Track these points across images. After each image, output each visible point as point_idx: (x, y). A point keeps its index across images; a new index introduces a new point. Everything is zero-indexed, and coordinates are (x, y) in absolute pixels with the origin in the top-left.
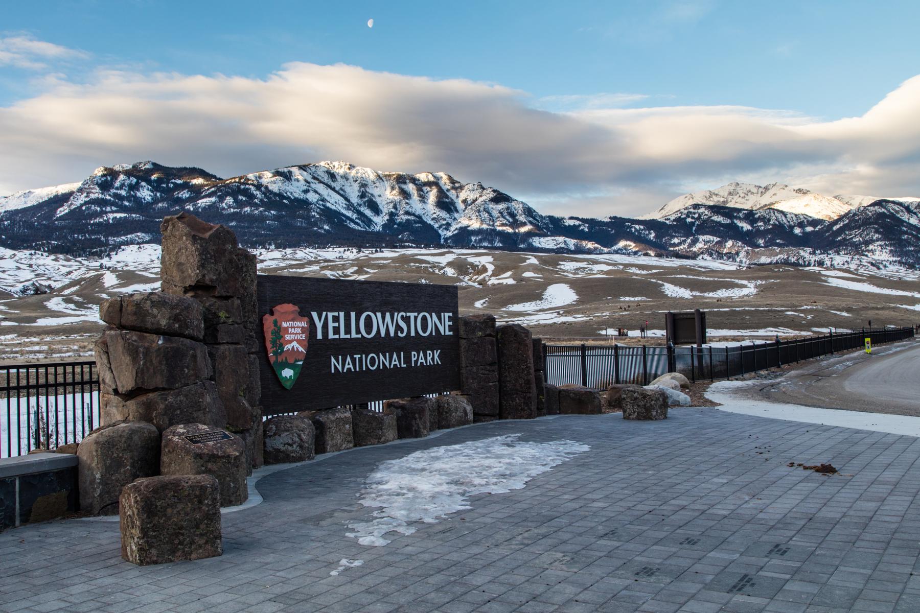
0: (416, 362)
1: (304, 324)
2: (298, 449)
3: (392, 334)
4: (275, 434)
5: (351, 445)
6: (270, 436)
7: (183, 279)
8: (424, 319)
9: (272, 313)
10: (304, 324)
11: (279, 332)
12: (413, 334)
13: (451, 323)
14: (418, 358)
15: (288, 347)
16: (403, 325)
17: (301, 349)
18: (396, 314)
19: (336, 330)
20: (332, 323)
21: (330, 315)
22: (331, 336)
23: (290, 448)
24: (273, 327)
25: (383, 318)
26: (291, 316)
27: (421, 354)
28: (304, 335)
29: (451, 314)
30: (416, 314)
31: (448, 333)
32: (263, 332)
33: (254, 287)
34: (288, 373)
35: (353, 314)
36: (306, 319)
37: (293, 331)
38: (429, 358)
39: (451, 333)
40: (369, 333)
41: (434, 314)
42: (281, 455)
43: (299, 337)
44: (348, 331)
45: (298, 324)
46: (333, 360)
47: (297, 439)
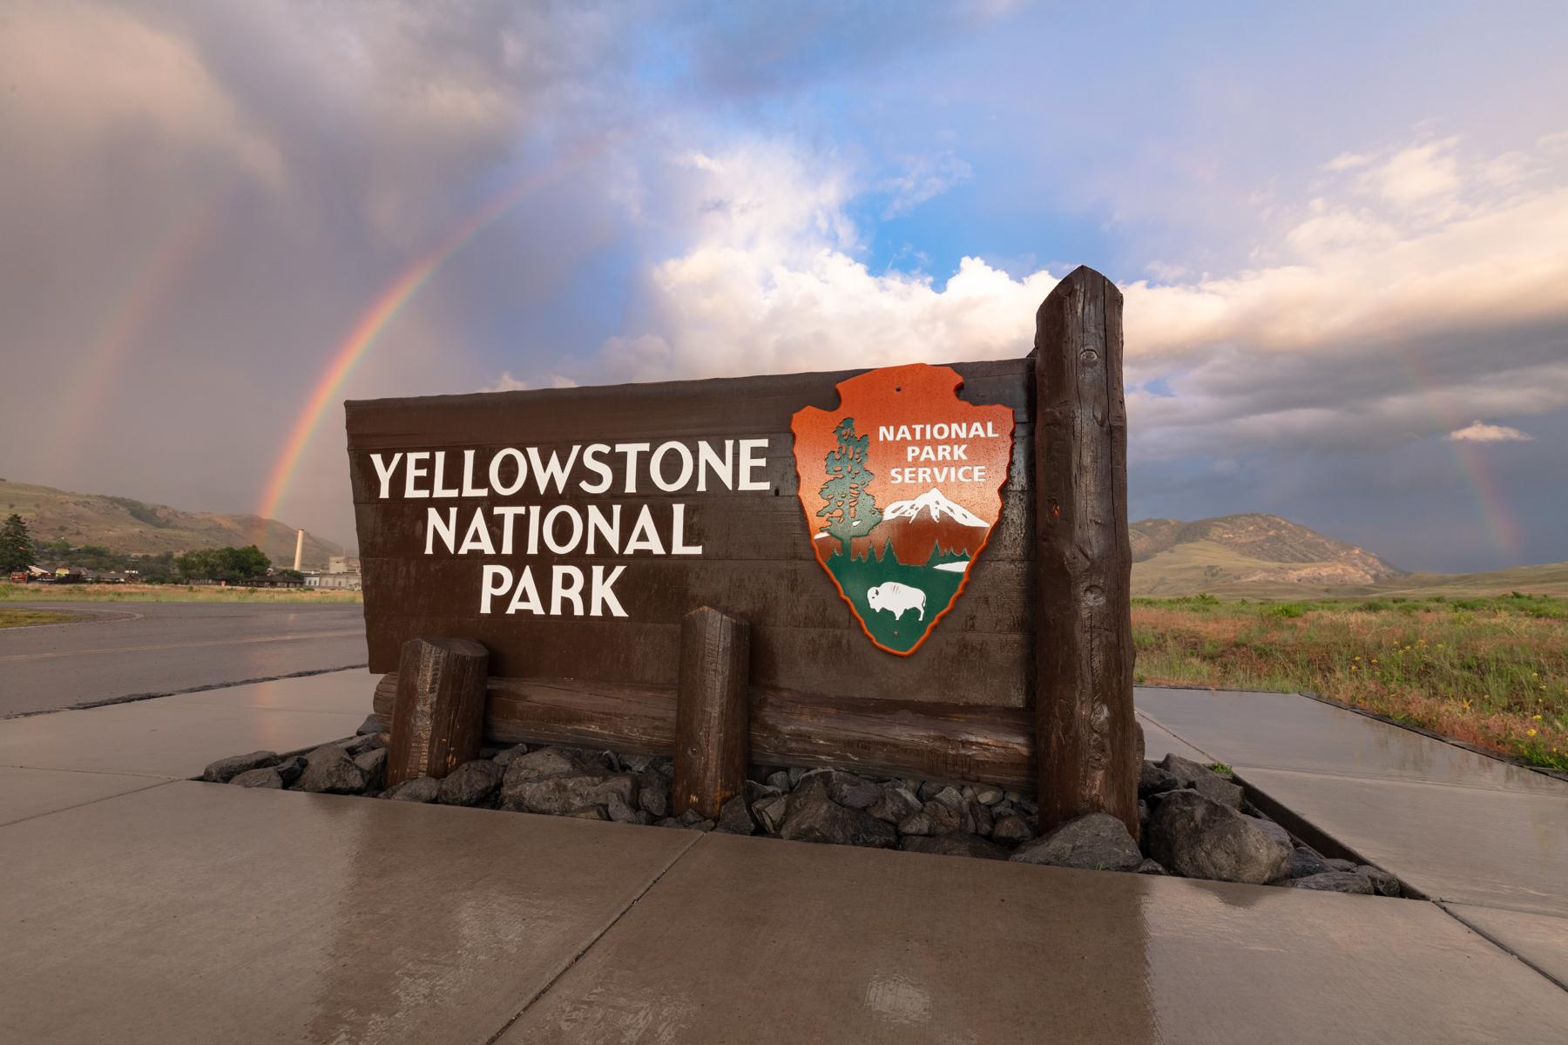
21: (412, 457)
22: (410, 492)
30: (645, 447)
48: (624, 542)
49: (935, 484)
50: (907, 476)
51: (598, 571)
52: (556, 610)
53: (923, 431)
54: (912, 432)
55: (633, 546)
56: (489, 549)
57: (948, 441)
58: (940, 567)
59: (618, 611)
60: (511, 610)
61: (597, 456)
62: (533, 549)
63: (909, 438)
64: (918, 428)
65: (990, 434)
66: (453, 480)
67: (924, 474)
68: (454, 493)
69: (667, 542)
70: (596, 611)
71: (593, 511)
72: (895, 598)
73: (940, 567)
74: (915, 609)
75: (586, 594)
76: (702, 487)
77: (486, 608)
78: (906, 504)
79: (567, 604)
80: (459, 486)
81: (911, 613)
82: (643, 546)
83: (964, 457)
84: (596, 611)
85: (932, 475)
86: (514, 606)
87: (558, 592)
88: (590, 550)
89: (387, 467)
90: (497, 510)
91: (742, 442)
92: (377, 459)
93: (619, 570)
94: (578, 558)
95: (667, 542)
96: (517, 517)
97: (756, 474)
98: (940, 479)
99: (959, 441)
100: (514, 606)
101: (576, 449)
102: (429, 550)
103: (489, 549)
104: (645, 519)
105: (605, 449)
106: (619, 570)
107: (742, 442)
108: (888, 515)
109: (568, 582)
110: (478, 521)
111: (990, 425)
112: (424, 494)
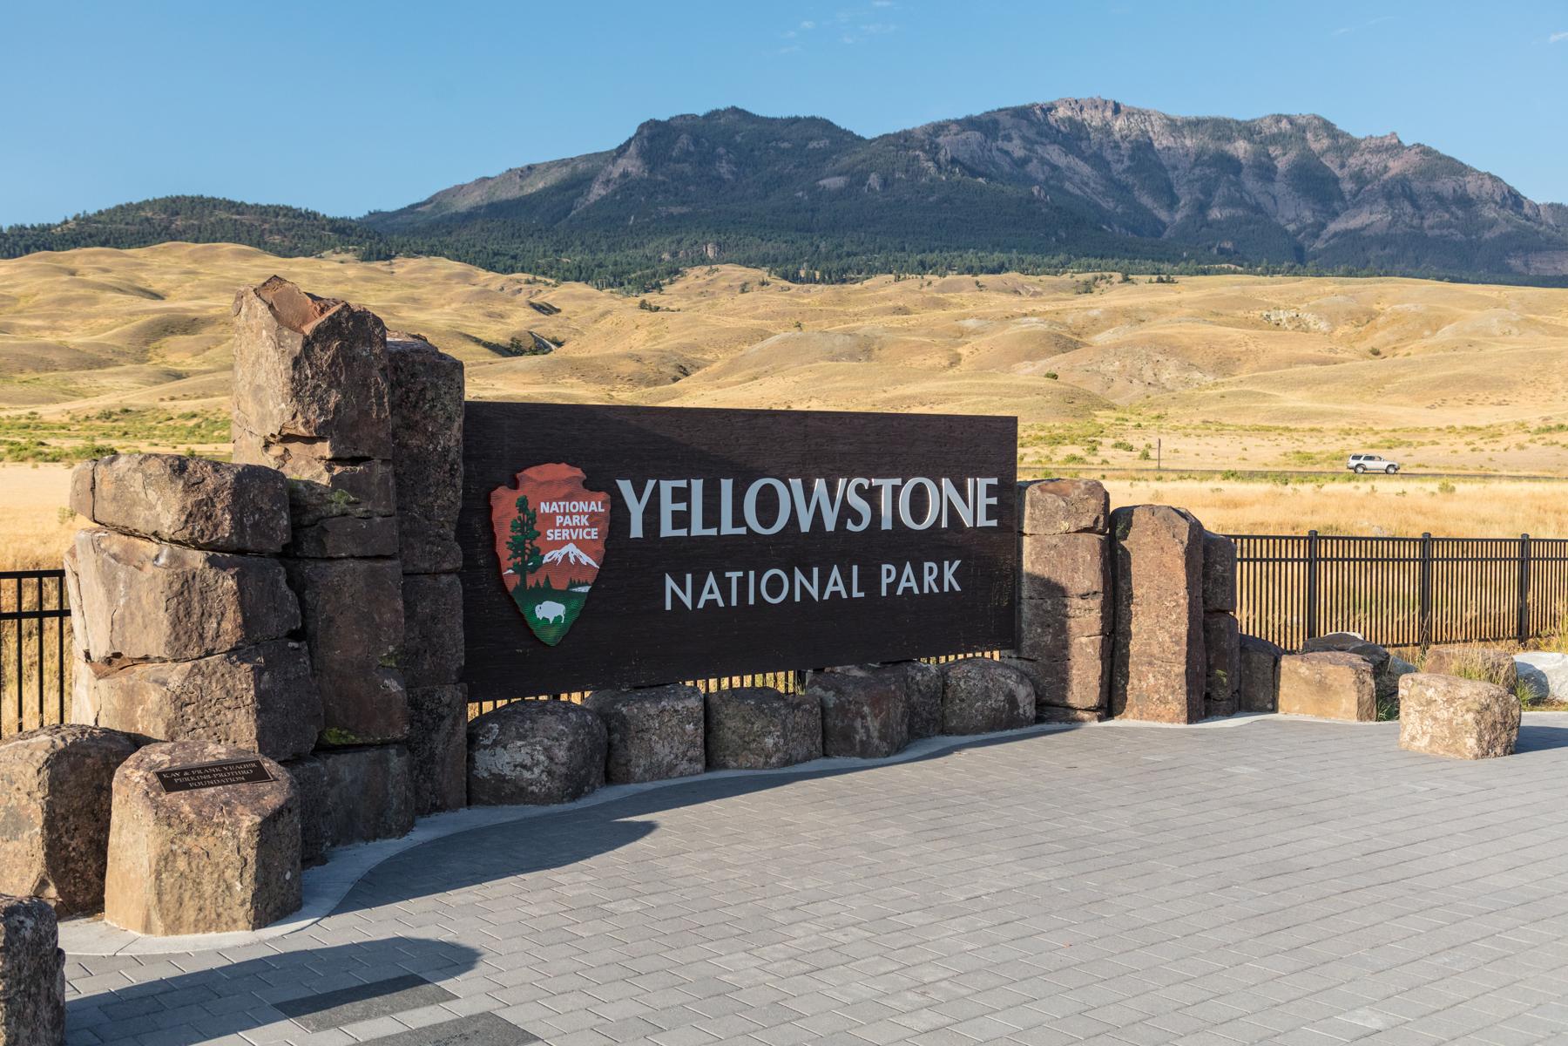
0: (893, 587)
1: (597, 506)
2: (544, 776)
3: (830, 526)
4: (495, 743)
5: (699, 767)
6: (485, 747)
7: (262, 420)
8: (919, 492)
9: (514, 484)
10: (597, 506)
11: (530, 525)
12: (887, 525)
13: (994, 501)
14: (896, 578)
15: (557, 555)
16: (861, 506)
17: (585, 559)
18: (841, 482)
19: (681, 520)
20: (669, 506)
21: (666, 487)
22: (667, 530)
23: (527, 775)
24: (515, 514)
25: (808, 491)
26: (566, 490)
27: (908, 569)
28: (594, 531)
29: (994, 481)
30: (898, 481)
31: (982, 521)
32: (490, 525)
33: (453, 436)
34: (550, 611)
35: (727, 486)
36: (603, 495)
37: (567, 521)
38: (929, 580)
39: (994, 523)
40: (767, 521)
41: (945, 482)
42: (508, 789)
43: (583, 534)
44: (712, 517)
45: (582, 506)
46: (670, 583)
47: (542, 758)
76: (944, 524)
80: (718, 525)
89: (639, 499)
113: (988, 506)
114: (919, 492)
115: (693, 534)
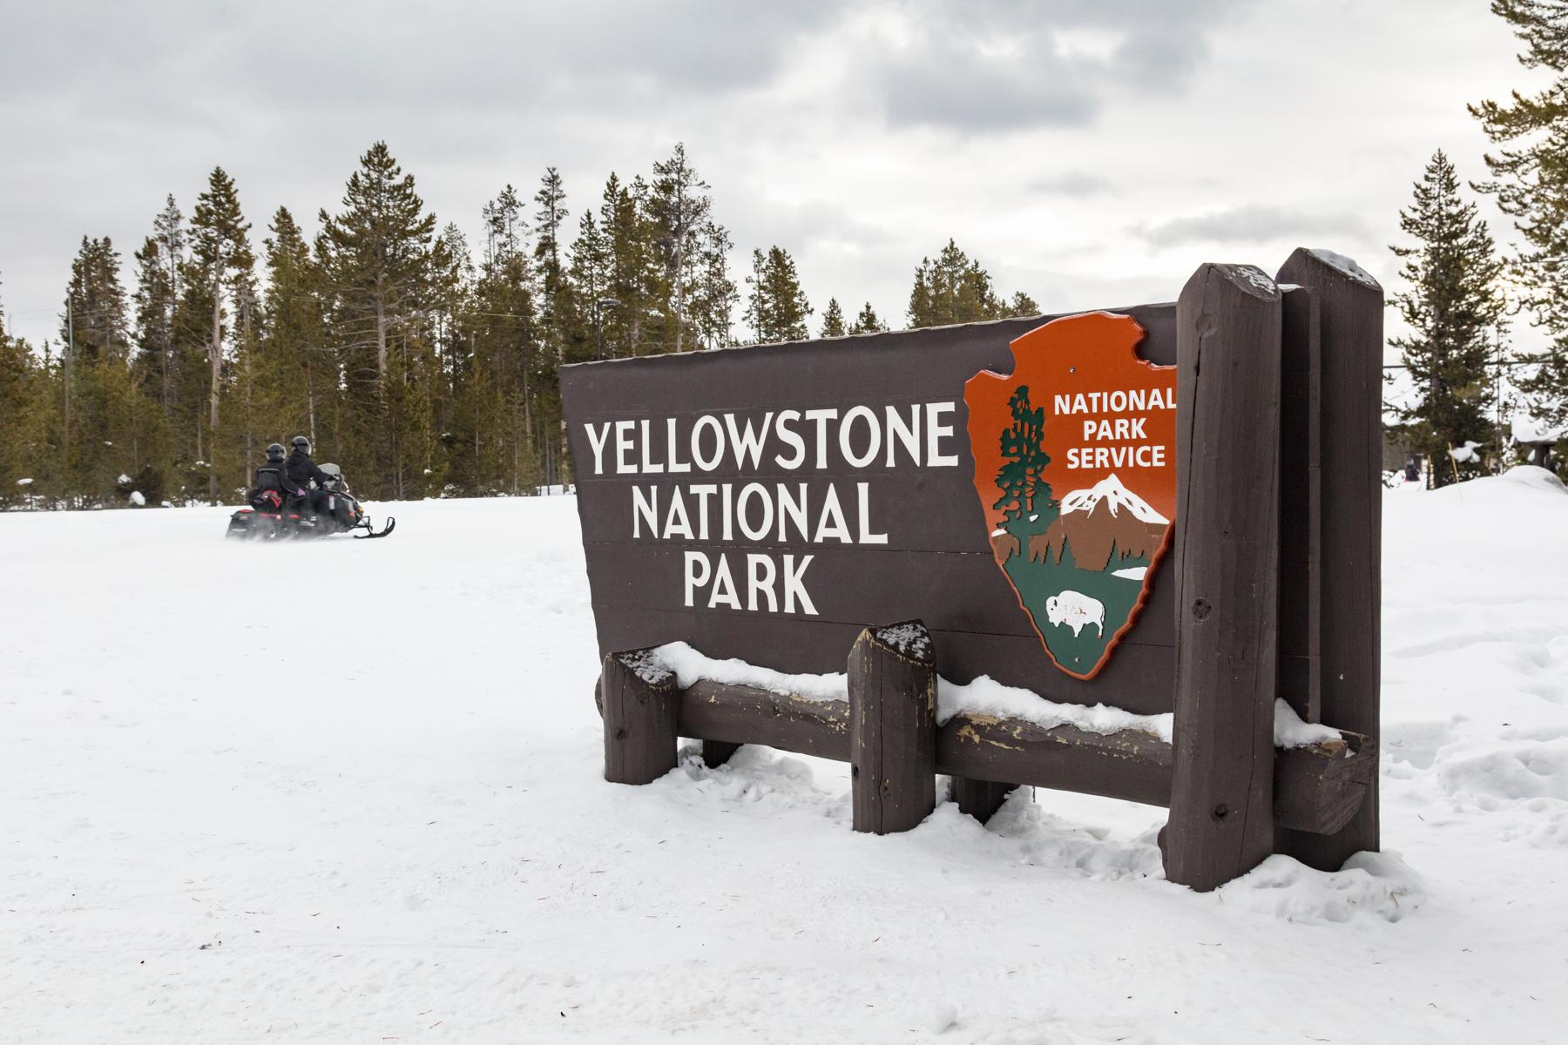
19: (633, 457)
21: (622, 426)
29: (950, 407)
30: (833, 414)
48: (813, 528)
49: (1113, 469)
50: (1085, 458)
51: (788, 560)
52: (753, 606)
53: (1100, 400)
54: (1089, 402)
55: (823, 533)
56: (689, 536)
57: (1127, 414)
58: (1119, 573)
59: (810, 609)
60: (712, 605)
61: (789, 425)
62: (728, 535)
63: (1086, 411)
64: (1094, 396)
65: (1171, 406)
66: (659, 455)
67: (1102, 456)
68: (659, 469)
69: (854, 529)
70: (790, 608)
71: (782, 488)
72: (1074, 610)
73: (1119, 573)
74: (1093, 624)
75: (779, 587)
77: (689, 601)
78: (1083, 494)
79: (761, 595)
81: (1089, 628)
82: (831, 533)
83: (1143, 436)
84: (790, 608)
85: (1110, 458)
86: (715, 599)
87: (753, 584)
88: (782, 538)
90: (694, 489)
91: (929, 406)
92: (589, 428)
93: (808, 559)
94: (770, 546)
95: (854, 529)
96: (710, 495)
97: (943, 451)
98: (1118, 464)
99: (1137, 414)
100: (715, 599)
101: (769, 416)
102: (637, 535)
103: (689, 536)
104: (832, 502)
105: (795, 415)
106: (808, 559)
107: (929, 406)
108: (1066, 508)
109: (762, 572)
110: (677, 503)
111: (1169, 391)
112: (633, 469)
113: (942, 440)
114: (860, 426)
115: (645, 470)
